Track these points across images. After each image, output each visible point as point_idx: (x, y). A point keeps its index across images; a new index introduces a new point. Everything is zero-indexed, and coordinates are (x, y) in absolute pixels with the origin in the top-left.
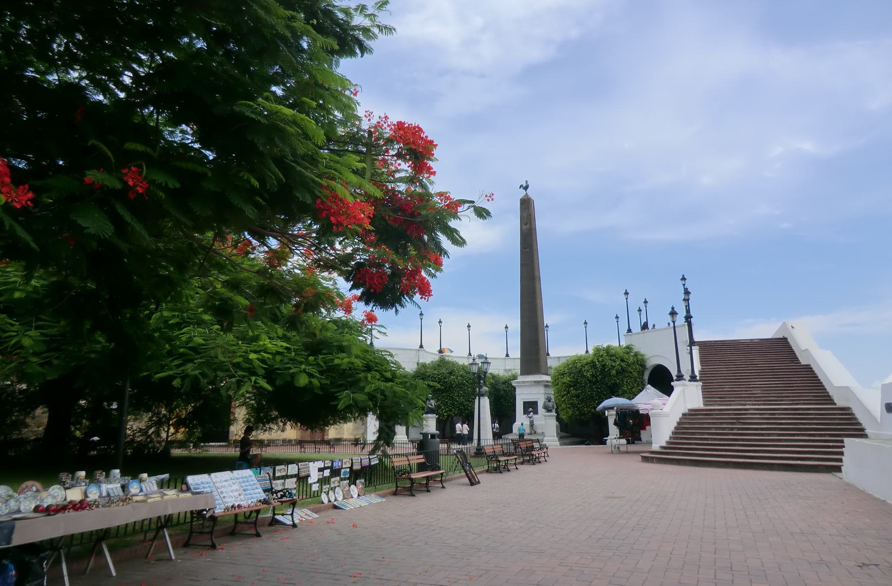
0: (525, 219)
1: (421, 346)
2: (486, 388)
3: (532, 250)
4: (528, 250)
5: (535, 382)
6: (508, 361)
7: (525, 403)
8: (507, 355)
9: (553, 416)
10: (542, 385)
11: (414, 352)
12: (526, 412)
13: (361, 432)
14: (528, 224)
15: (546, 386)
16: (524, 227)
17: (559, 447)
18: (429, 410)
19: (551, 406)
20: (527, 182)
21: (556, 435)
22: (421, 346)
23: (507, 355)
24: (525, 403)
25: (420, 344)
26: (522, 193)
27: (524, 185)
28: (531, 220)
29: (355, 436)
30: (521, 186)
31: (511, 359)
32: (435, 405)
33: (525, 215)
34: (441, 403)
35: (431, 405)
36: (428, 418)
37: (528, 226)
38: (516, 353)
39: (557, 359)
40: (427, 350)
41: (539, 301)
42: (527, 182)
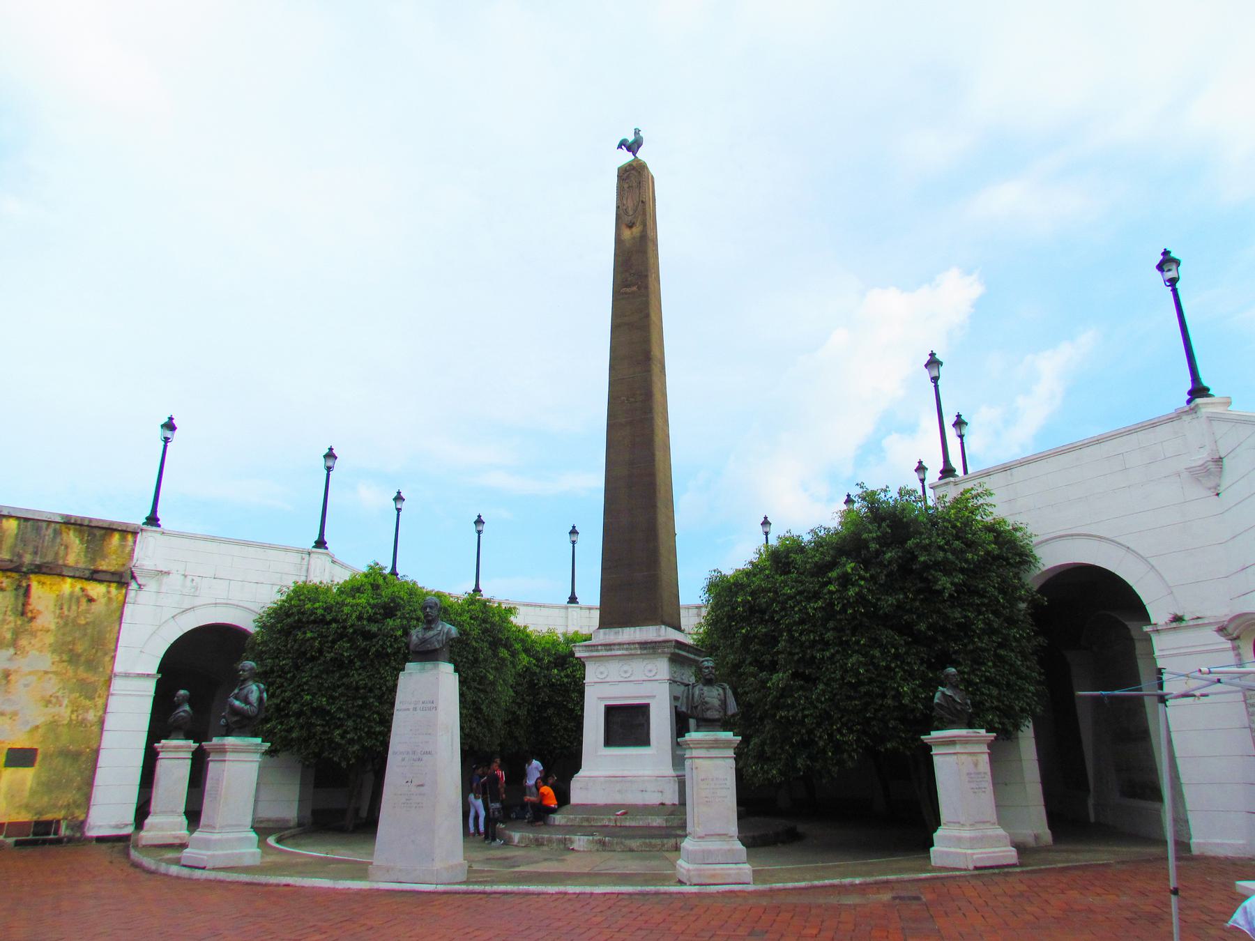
0: (631, 213)
1: (321, 543)
2: (448, 626)
3: (646, 287)
4: (635, 288)
5: (644, 645)
6: (574, 612)
7: (611, 712)
8: (573, 599)
9: (724, 744)
10: (663, 653)
11: (296, 558)
12: (611, 739)
13: (70, 796)
14: (638, 224)
15: (675, 660)
16: (627, 234)
17: (751, 888)
18: (235, 719)
19: (716, 702)
20: (637, 132)
21: (733, 829)
22: (321, 543)
23: (573, 599)
24: (611, 712)
25: (316, 538)
26: (626, 157)
27: (631, 138)
28: (644, 213)
29: (40, 813)
30: (623, 144)
31: (581, 608)
32: (260, 699)
33: (630, 204)
34: (340, 709)
35: (246, 700)
36: (222, 750)
37: (636, 230)
38: (591, 593)
39: (695, 611)
40: (337, 557)
41: (658, 421)
42: (637, 132)
